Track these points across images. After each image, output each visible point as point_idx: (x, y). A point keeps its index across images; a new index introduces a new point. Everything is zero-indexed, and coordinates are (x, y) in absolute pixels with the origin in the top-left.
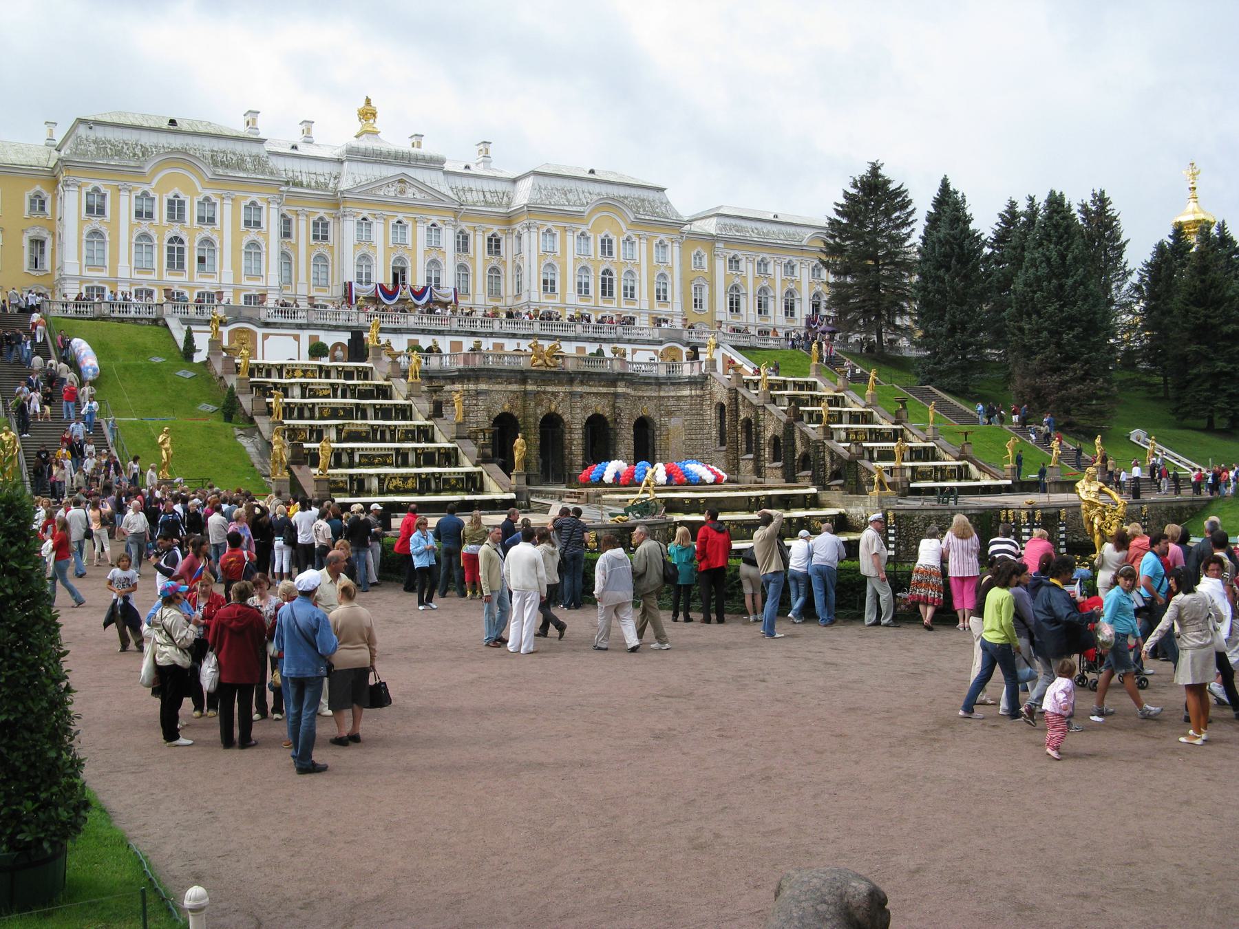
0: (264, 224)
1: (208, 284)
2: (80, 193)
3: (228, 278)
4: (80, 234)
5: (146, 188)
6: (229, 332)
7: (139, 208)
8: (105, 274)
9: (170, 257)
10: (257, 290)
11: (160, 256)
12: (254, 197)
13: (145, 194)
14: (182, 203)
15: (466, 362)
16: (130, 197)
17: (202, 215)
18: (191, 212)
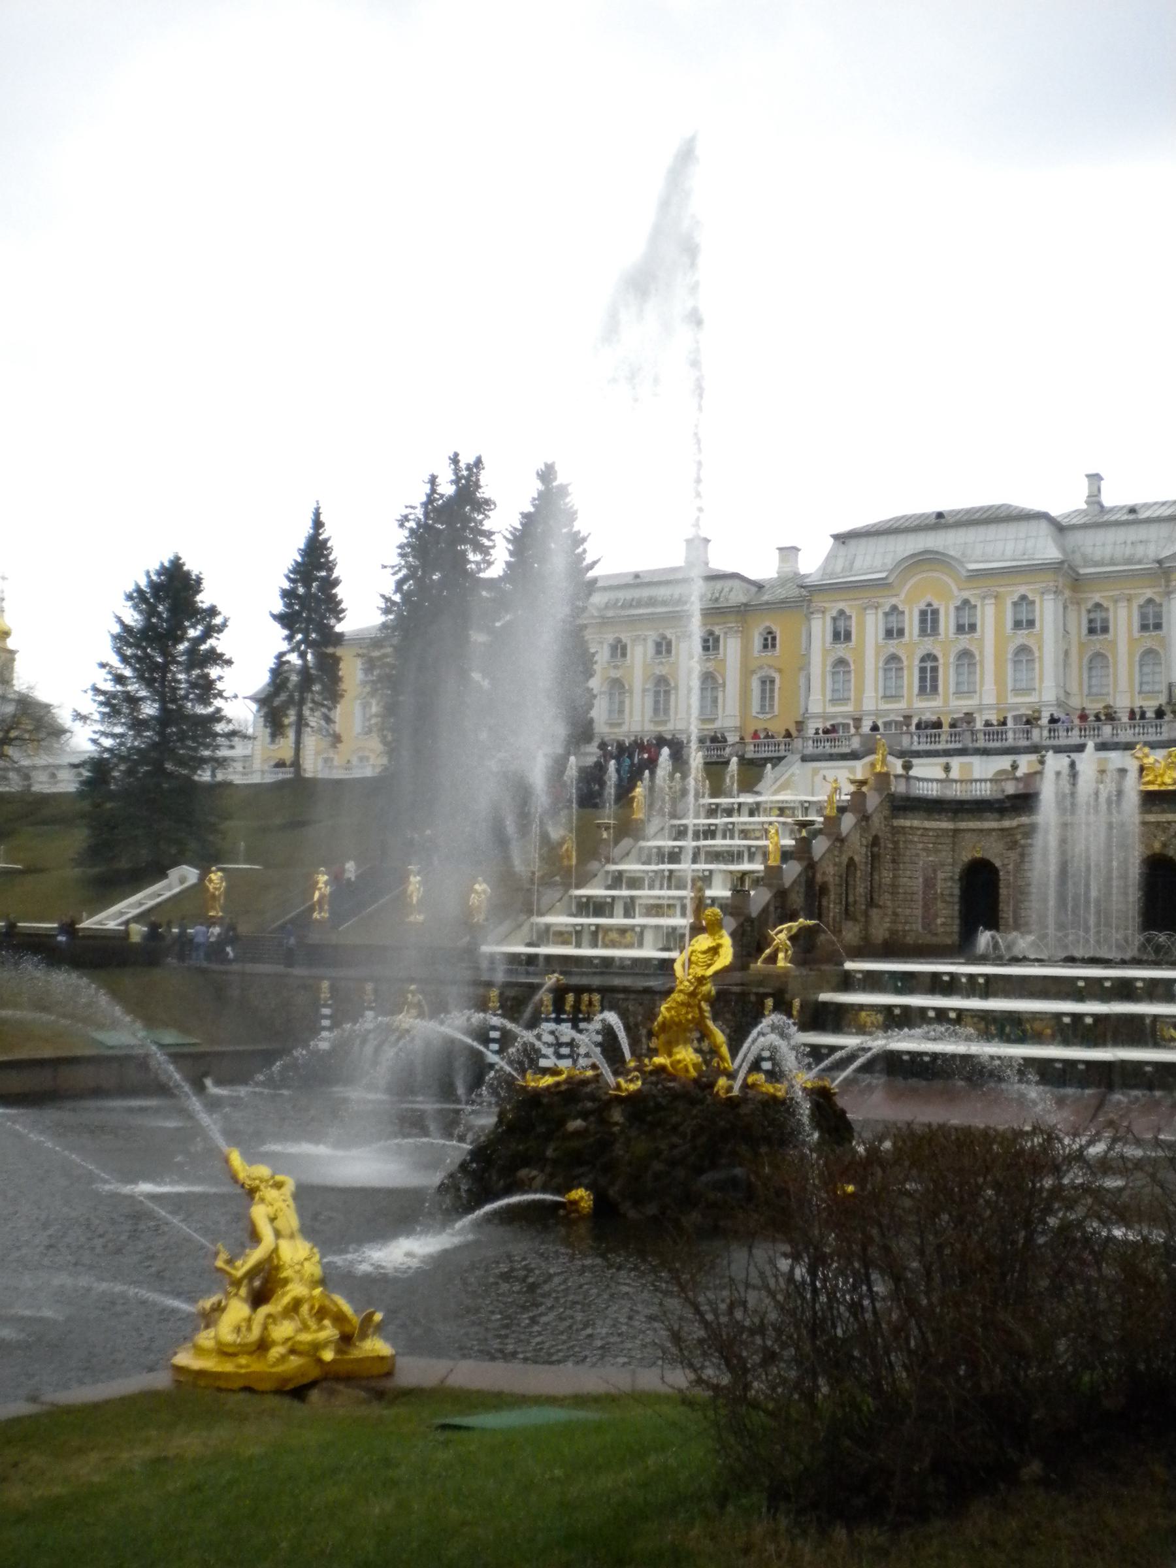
0: (1037, 624)
1: (960, 706)
2: (824, 618)
3: (989, 698)
4: (824, 665)
5: (894, 601)
6: (863, 766)
7: (890, 626)
8: (849, 708)
9: (922, 679)
10: (1028, 708)
11: (911, 678)
12: (1023, 590)
13: (894, 608)
14: (935, 612)
15: (1027, 785)
16: (876, 614)
17: (961, 622)
18: (947, 623)
